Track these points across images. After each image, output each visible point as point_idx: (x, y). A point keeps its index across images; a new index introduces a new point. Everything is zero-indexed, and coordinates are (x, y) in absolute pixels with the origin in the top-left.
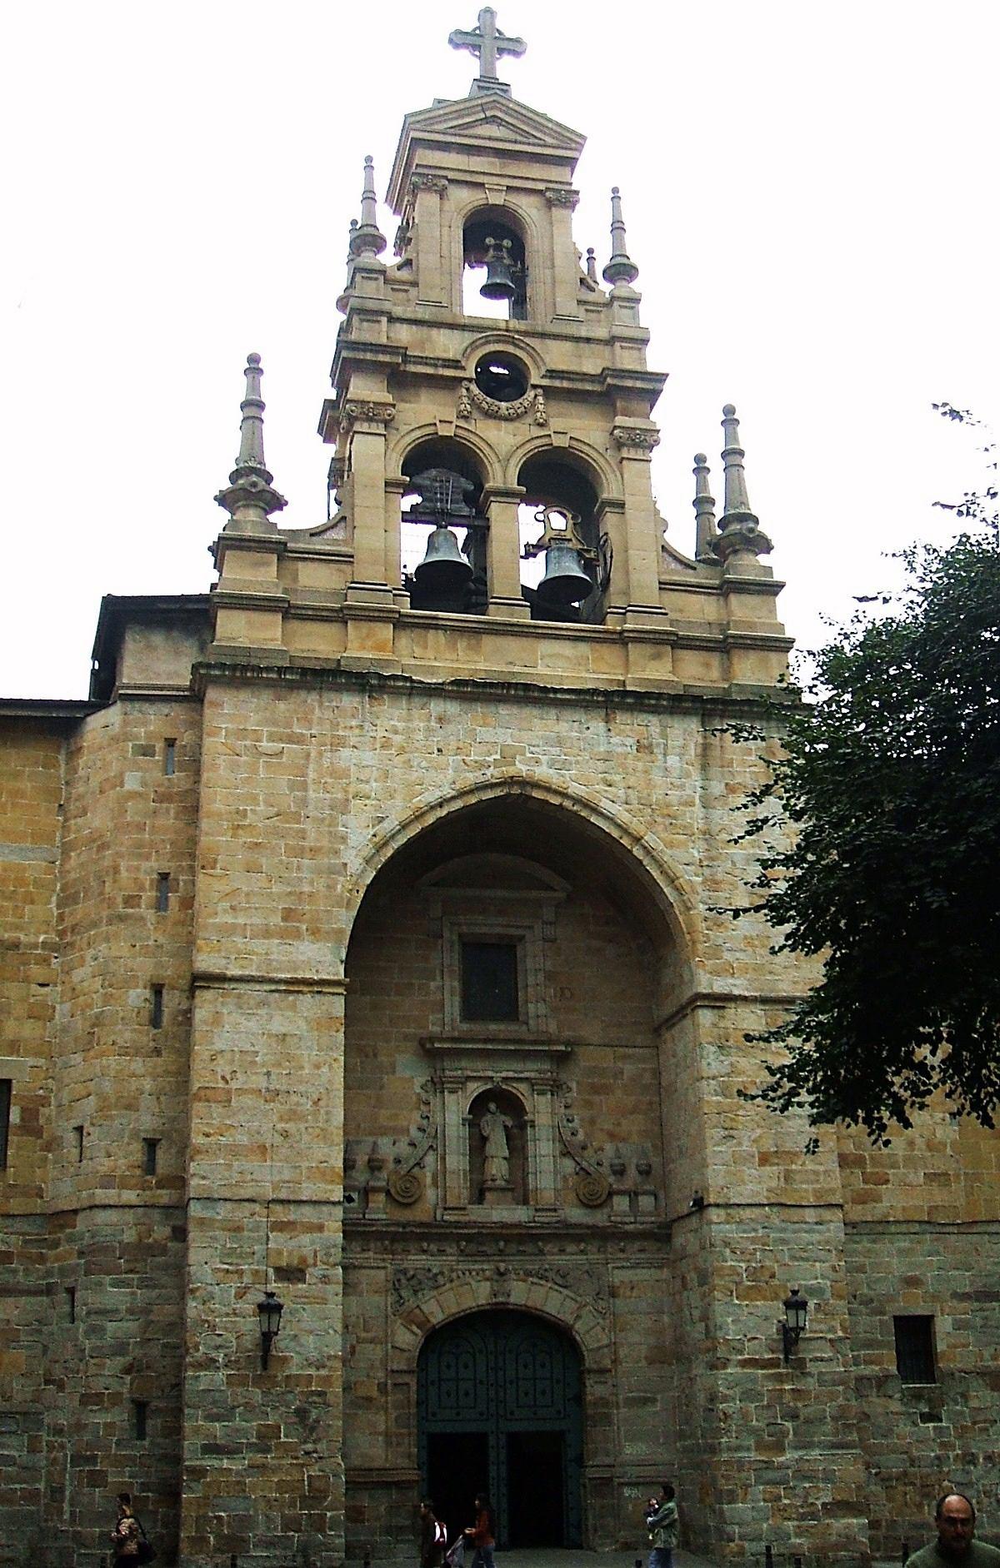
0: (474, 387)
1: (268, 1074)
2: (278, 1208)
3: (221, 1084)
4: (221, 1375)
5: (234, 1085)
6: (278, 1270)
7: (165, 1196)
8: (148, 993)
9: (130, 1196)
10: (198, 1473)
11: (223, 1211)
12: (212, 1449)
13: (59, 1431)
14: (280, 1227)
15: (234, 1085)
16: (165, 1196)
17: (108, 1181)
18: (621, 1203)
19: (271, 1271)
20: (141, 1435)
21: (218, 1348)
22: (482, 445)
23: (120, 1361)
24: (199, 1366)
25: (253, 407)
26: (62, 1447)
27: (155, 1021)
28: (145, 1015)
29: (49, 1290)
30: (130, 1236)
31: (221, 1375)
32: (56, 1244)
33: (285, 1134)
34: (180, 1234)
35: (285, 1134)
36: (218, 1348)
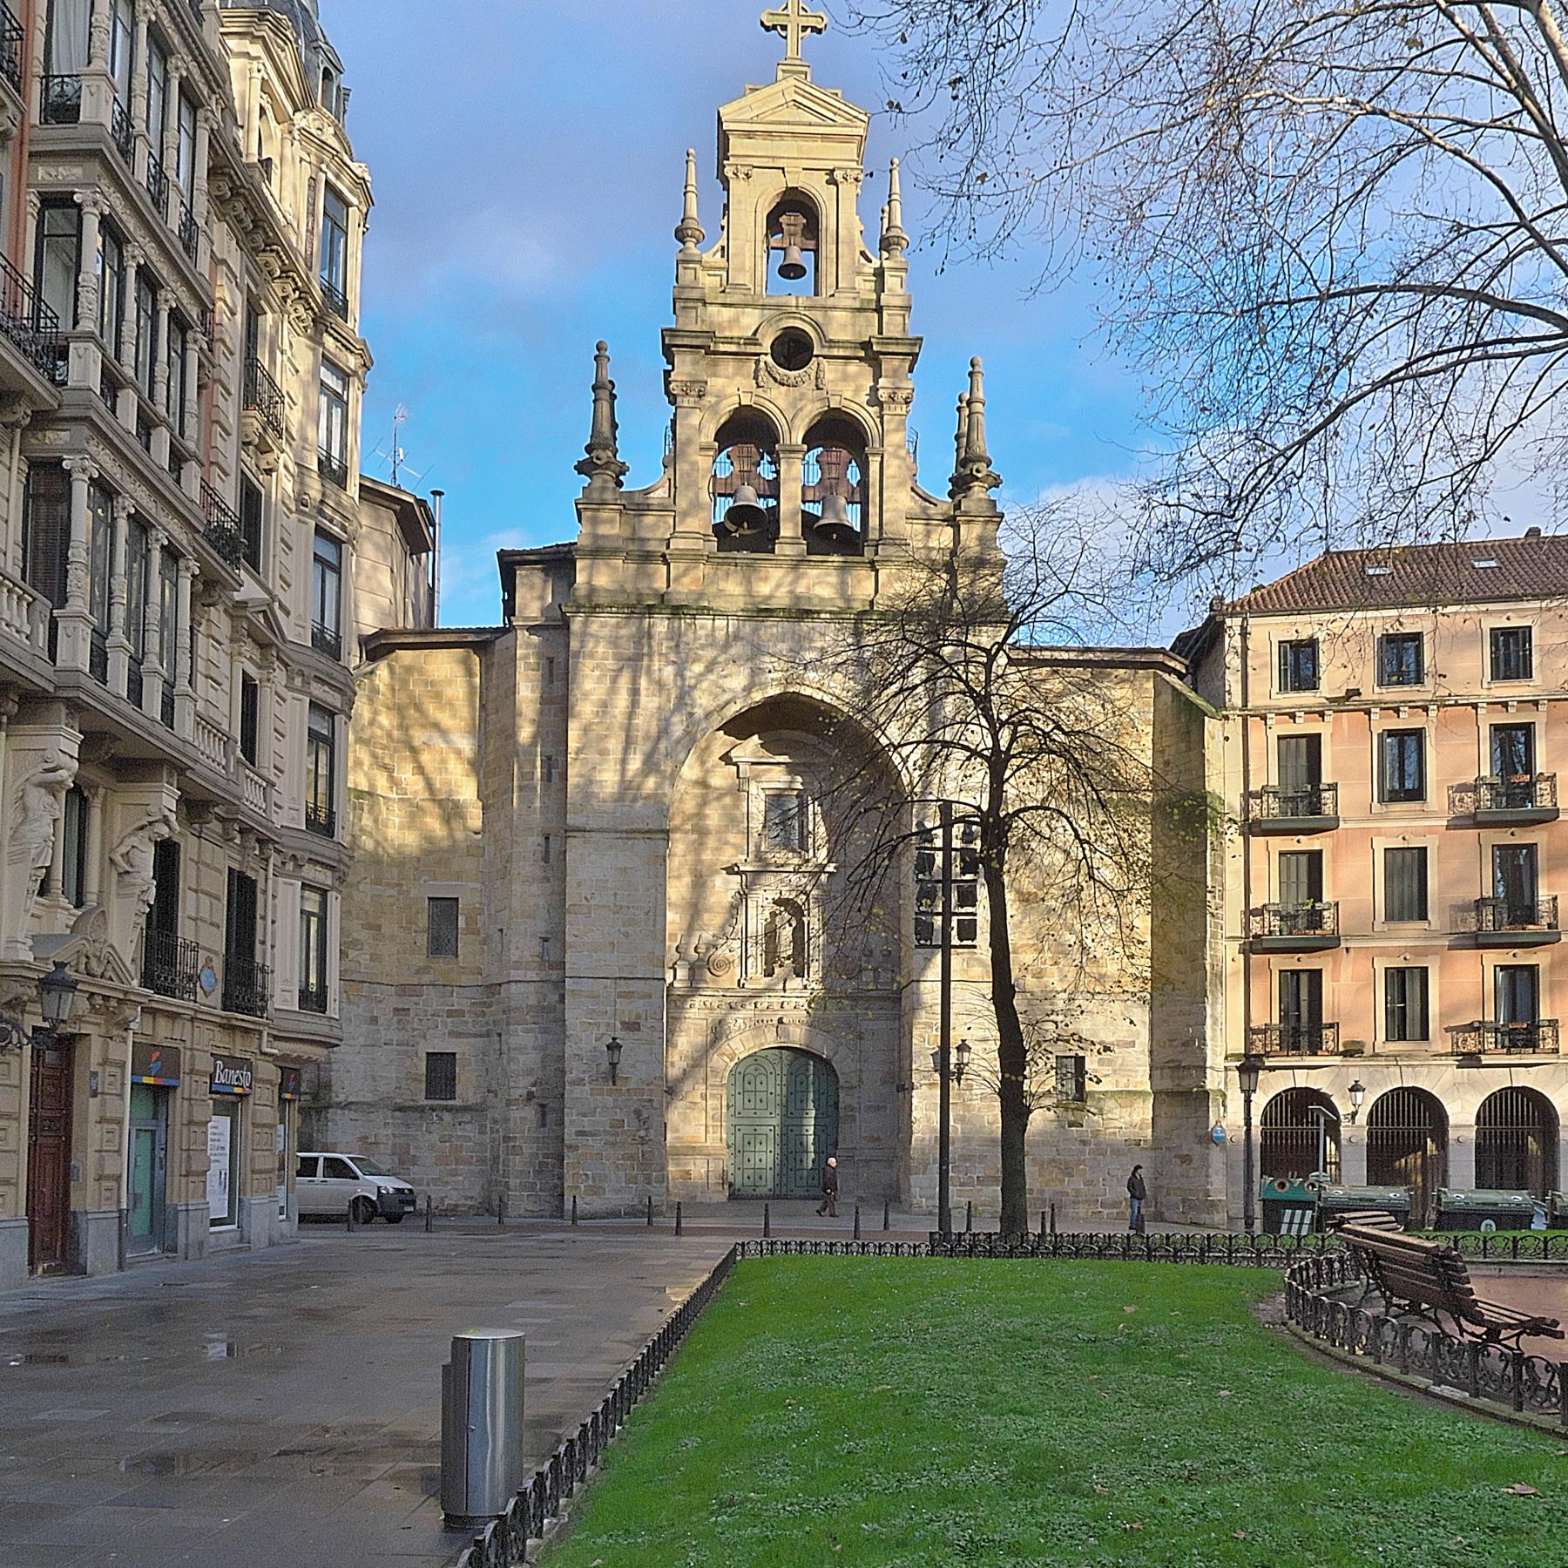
0: (769, 359)
1: (615, 894)
2: (622, 982)
3: (584, 902)
4: (587, 1087)
5: (593, 902)
6: (623, 1023)
7: (554, 975)
8: (541, 840)
9: (532, 975)
10: (575, 1148)
11: (586, 985)
12: (580, 1133)
13: (496, 1122)
14: (621, 995)
15: (593, 902)
16: (554, 975)
17: (518, 965)
18: (867, 976)
19: (618, 1024)
20: (544, 1125)
21: (584, 1072)
22: (777, 411)
23: (532, 1079)
24: (573, 1083)
25: (603, 390)
26: (498, 1131)
27: (546, 859)
28: (539, 856)
29: (488, 1035)
30: (532, 1001)
31: (587, 1087)
32: (490, 1006)
33: (627, 935)
34: (562, 999)
35: (627, 935)
36: (584, 1072)
